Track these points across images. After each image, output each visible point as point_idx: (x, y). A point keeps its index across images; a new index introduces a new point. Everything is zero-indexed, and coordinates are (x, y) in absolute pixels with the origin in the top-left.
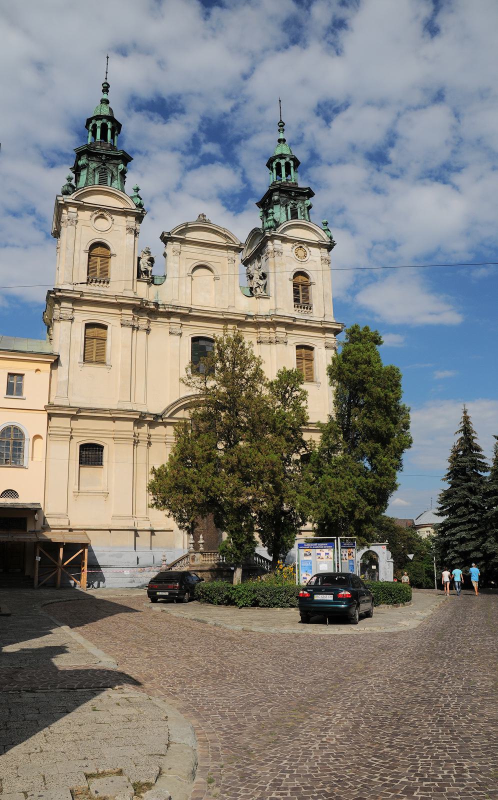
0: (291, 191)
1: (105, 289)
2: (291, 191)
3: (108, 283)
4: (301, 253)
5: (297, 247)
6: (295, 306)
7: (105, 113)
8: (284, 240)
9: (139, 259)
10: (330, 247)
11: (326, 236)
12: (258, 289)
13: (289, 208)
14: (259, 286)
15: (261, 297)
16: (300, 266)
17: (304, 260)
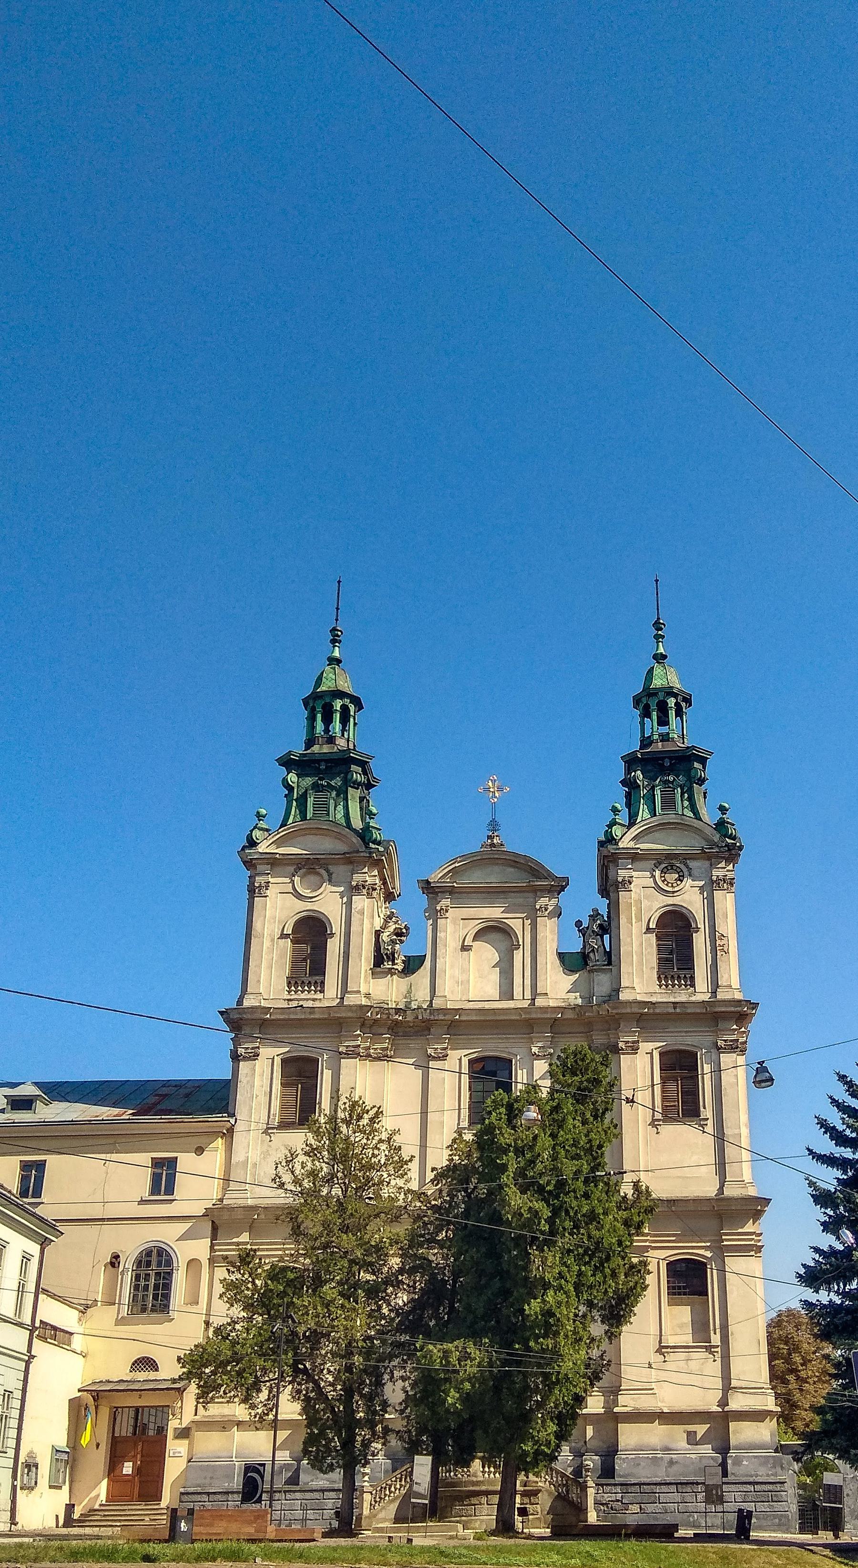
0: (663, 759)
1: (319, 996)
2: (663, 759)
3: (323, 983)
4: (672, 877)
5: (664, 865)
6: (659, 978)
7: (330, 684)
8: (635, 857)
9: (378, 934)
10: (731, 853)
11: (718, 836)
12: (591, 955)
13: (658, 792)
14: (593, 950)
15: (596, 970)
16: (671, 901)
17: (676, 889)
